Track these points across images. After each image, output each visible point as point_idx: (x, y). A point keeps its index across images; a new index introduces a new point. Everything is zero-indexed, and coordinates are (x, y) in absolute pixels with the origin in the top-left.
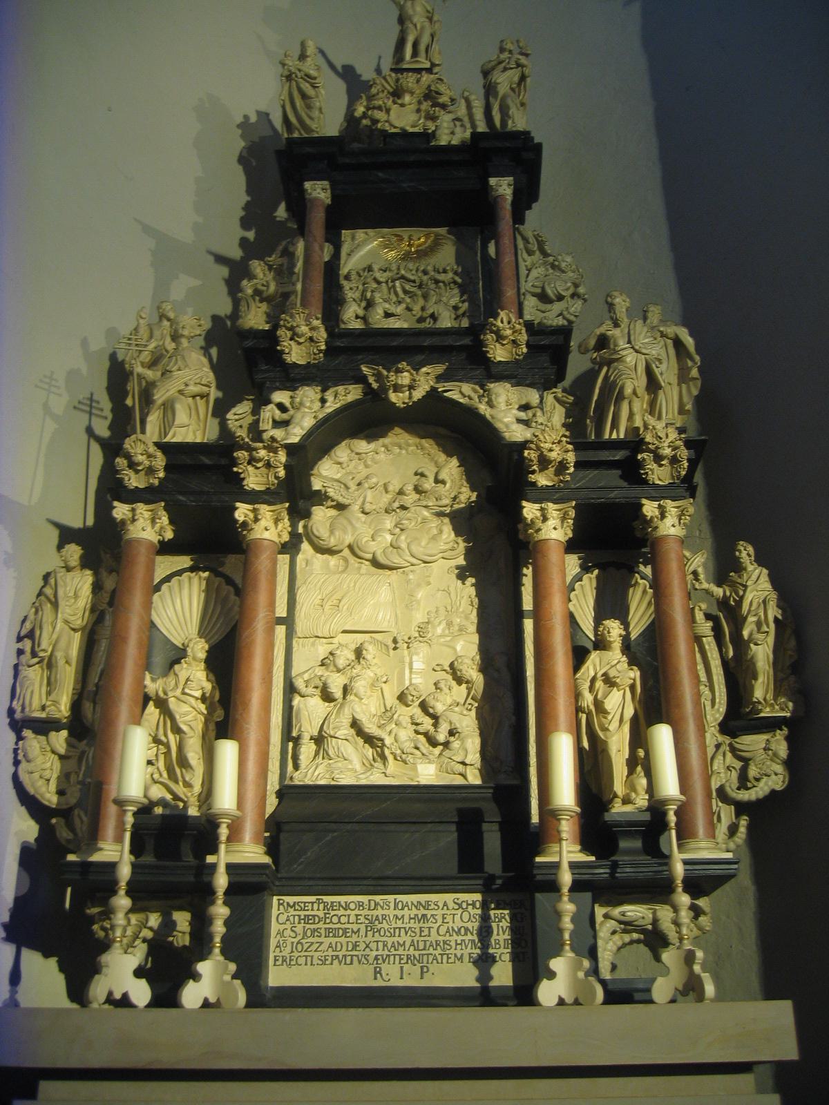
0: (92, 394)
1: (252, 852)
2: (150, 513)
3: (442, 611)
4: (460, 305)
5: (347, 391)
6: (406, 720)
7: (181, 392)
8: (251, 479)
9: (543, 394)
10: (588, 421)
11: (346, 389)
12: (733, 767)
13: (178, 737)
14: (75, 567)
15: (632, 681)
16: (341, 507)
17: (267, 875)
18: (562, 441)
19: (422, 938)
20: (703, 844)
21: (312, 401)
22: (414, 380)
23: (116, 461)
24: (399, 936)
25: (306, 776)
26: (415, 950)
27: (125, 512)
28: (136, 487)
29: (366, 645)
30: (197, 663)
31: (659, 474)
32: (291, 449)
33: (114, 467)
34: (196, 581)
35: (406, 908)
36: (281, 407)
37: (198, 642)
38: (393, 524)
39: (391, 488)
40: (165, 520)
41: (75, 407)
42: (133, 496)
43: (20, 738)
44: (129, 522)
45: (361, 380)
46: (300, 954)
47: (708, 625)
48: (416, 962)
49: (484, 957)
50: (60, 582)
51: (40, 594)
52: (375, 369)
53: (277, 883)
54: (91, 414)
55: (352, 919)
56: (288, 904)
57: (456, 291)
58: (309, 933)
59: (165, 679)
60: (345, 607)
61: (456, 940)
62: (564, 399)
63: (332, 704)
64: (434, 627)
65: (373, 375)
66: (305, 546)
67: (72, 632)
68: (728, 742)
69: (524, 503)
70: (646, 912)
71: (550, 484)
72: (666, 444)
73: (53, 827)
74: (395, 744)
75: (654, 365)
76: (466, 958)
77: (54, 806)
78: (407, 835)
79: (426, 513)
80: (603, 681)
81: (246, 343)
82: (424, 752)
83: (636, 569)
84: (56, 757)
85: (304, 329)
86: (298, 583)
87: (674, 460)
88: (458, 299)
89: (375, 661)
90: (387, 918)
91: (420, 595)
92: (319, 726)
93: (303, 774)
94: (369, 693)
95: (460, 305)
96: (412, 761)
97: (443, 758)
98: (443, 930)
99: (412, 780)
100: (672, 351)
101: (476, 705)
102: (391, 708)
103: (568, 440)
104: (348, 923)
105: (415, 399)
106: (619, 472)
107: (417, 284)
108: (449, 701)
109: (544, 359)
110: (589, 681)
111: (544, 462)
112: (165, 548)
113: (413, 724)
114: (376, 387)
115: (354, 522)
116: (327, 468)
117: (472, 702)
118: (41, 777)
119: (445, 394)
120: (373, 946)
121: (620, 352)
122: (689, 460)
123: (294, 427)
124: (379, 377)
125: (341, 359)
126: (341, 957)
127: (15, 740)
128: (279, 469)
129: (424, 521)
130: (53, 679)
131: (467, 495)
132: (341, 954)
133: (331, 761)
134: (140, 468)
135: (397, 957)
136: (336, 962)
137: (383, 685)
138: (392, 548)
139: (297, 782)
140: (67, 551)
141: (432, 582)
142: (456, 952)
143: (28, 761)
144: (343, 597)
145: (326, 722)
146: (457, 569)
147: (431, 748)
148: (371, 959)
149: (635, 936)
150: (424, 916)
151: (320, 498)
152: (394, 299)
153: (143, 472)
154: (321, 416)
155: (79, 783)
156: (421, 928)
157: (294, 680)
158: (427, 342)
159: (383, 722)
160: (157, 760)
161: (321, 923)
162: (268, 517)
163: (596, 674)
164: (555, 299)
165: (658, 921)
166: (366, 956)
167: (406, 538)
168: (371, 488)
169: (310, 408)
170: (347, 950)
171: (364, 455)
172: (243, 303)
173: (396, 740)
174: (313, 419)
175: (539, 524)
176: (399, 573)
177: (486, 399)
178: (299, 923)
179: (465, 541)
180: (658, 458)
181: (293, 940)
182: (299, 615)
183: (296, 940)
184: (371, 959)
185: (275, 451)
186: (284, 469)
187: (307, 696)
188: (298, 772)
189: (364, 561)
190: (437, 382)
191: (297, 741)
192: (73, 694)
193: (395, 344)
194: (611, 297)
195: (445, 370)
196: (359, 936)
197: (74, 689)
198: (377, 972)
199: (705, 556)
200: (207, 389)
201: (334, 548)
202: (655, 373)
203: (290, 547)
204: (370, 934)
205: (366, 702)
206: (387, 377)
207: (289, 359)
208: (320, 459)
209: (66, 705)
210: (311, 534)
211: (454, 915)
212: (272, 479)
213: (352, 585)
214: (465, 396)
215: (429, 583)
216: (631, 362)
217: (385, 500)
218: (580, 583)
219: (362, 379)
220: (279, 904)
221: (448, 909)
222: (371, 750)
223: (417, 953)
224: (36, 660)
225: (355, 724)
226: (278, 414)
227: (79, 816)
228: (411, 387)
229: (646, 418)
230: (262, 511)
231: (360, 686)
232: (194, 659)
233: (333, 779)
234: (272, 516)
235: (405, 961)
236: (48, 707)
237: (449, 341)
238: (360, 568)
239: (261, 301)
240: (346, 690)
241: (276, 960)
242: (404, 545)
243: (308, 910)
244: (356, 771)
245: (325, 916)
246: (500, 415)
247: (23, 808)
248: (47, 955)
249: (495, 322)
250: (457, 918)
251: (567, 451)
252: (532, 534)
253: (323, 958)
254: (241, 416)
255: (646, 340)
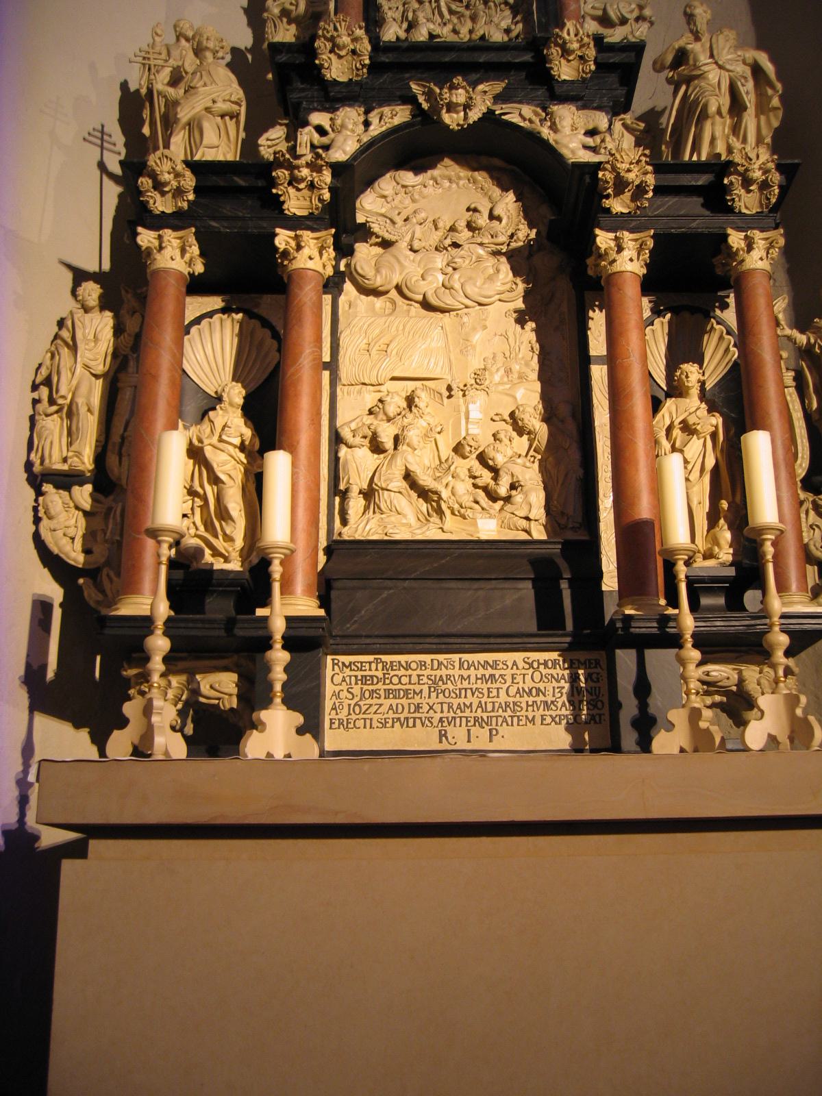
0: (103, 126)
1: (306, 606)
2: (178, 241)
3: (500, 358)
4: (513, 27)
5: (394, 113)
6: (463, 473)
7: (207, 109)
8: (292, 202)
9: (612, 118)
10: (663, 147)
11: (393, 110)
12: (817, 526)
13: (215, 488)
14: (93, 308)
15: (714, 429)
16: (386, 244)
17: (323, 629)
18: (641, 161)
19: (490, 700)
20: (796, 599)
21: (355, 124)
22: (471, 98)
23: (139, 181)
24: (466, 697)
25: (356, 531)
26: (483, 712)
27: (151, 239)
28: (163, 212)
29: (418, 392)
30: (234, 409)
31: (747, 202)
32: (338, 169)
33: (137, 188)
34: (228, 323)
35: (472, 668)
36: (321, 131)
37: (235, 386)
38: (445, 263)
39: (441, 225)
40: (195, 250)
41: (84, 139)
42: (158, 222)
43: (39, 493)
44: (155, 251)
46: (357, 717)
47: (790, 374)
48: (484, 725)
49: (557, 719)
50: (77, 323)
51: (56, 337)
52: (424, 86)
53: (332, 641)
54: (102, 147)
55: (415, 679)
56: (343, 663)
57: (508, 12)
58: (367, 695)
59: (199, 426)
60: (394, 352)
61: (527, 702)
62: (635, 125)
63: (382, 456)
64: (492, 374)
65: (424, 93)
66: (348, 286)
67: (94, 379)
68: (811, 499)
69: (598, 231)
70: (732, 672)
71: (625, 211)
72: (756, 166)
73: (80, 588)
74: (453, 497)
75: (739, 84)
76: (538, 720)
77: (80, 566)
78: (470, 592)
79: (481, 251)
80: (681, 429)
81: (279, 57)
82: (485, 506)
83: (712, 314)
84: (80, 513)
85: (345, 40)
86: (341, 326)
87: (764, 185)
88: (510, 21)
89: (428, 410)
90: (452, 679)
91: (477, 337)
92: (370, 476)
93: (354, 530)
94: (422, 444)
95: (513, 27)
96: (471, 515)
97: (504, 514)
98: (513, 691)
99: (472, 536)
101: (540, 457)
102: (446, 460)
103: (648, 160)
104: (410, 683)
105: (471, 122)
106: (701, 200)
107: (464, 4)
108: (509, 453)
109: (613, 79)
110: (664, 429)
111: (621, 185)
112: (196, 286)
113: (470, 477)
114: (426, 108)
115: (402, 259)
116: (370, 201)
117: (536, 455)
118: (65, 535)
119: (503, 117)
120: (437, 707)
121: (702, 68)
122: (780, 187)
123: (336, 151)
124: (430, 95)
125: (386, 77)
126: (402, 720)
127: (34, 497)
128: (324, 191)
129: (479, 259)
130: (74, 428)
131: (525, 233)
132: (402, 717)
133: (383, 516)
134: (166, 189)
135: (464, 720)
136: (397, 725)
137: (438, 436)
138: (443, 289)
139: (346, 538)
140: (84, 290)
141: (488, 325)
142: (526, 713)
143: (50, 518)
144: (391, 341)
145: (377, 474)
146: (515, 312)
147: (491, 503)
148: (435, 721)
149: (718, 698)
150: (492, 676)
151: (364, 232)
152: (439, 20)
153: (170, 195)
154: (365, 139)
155: (106, 541)
156: (488, 689)
157: (339, 430)
158: (483, 58)
159: (438, 474)
160: (193, 514)
161: (380, 684)
162: (312, 245)
163: (672, 423)
164: (617, 21)
165: (744, 681)
166: (430, 719)
167: (459, 280)
168: (421, 224)
169: (353, 131)
170: (409, 712)
171: (411, 188)
172: (270, 25)
173: (453, 494)
174: (356, 143)
175: (613, 255)
176: (452, 316)
177: (549, 124)
178: (356, 684)
179: (524, 281)
180: (747, 183)
181: (350, 702)
182: (343, 361)
183: (353, 702)
184: (435, 721)
185: (319, 170)
186: (329, 191)
187: (355, 447)
188: (347, 528)
189: (413, 303)
190: (495, 103)
191: (344, 495)
192: (96, 446)
193: (447, 59)
194: (690, 7)
195: (504, 89)
196: (421, 698)
197: (97, 441)
198: (443, 735)
199: (786, 301)
200: (236, 107)
201: (380, 288)
202: (741, 93)
203: (333, 285)
204: (433, 695)
205: (419, 454)
206: (440, 94)
207: (328, 76)
208: (363, 191)
209: (89, 458)
210: (354, 273)
211: (524, 675)
212: (315, 202)
213: (401, 328)
214: (524, 119)
215: (485, 327)
216: (714, 79)
217: (435, 237)
218: (650, 327)
219: (411, 100)
220: (334, 664)
221: (517, 668)
222: (425, 505)
223: (485, 716)
224: (55, 408)
225: (408, 476)
226: (316, 135)
227: (108, 575)
228: (467, 107)
229: (730, 141)
230: (305, 238)
231: (413, 435)
232: (231, 404)
233: (386, 534)
234: (317, 243)
235: (472, 723)
236: (70, 458)
237: (507, 57)
238: (409, 311)
239: (289, 23)
240: (397, 439)
241: (331, 723)
242: (457, 286)
243: (365, 670)
244: (411, 526)
245: (384, 676)
246: (565, 141)
247: (46, 570)
248: (77, 726)
249: (560, 33)
250: (528, 678)
251: (646, 173)
252: (605, 266)
253: (383, 721)
254: (277, 141)
255: (729, 57)
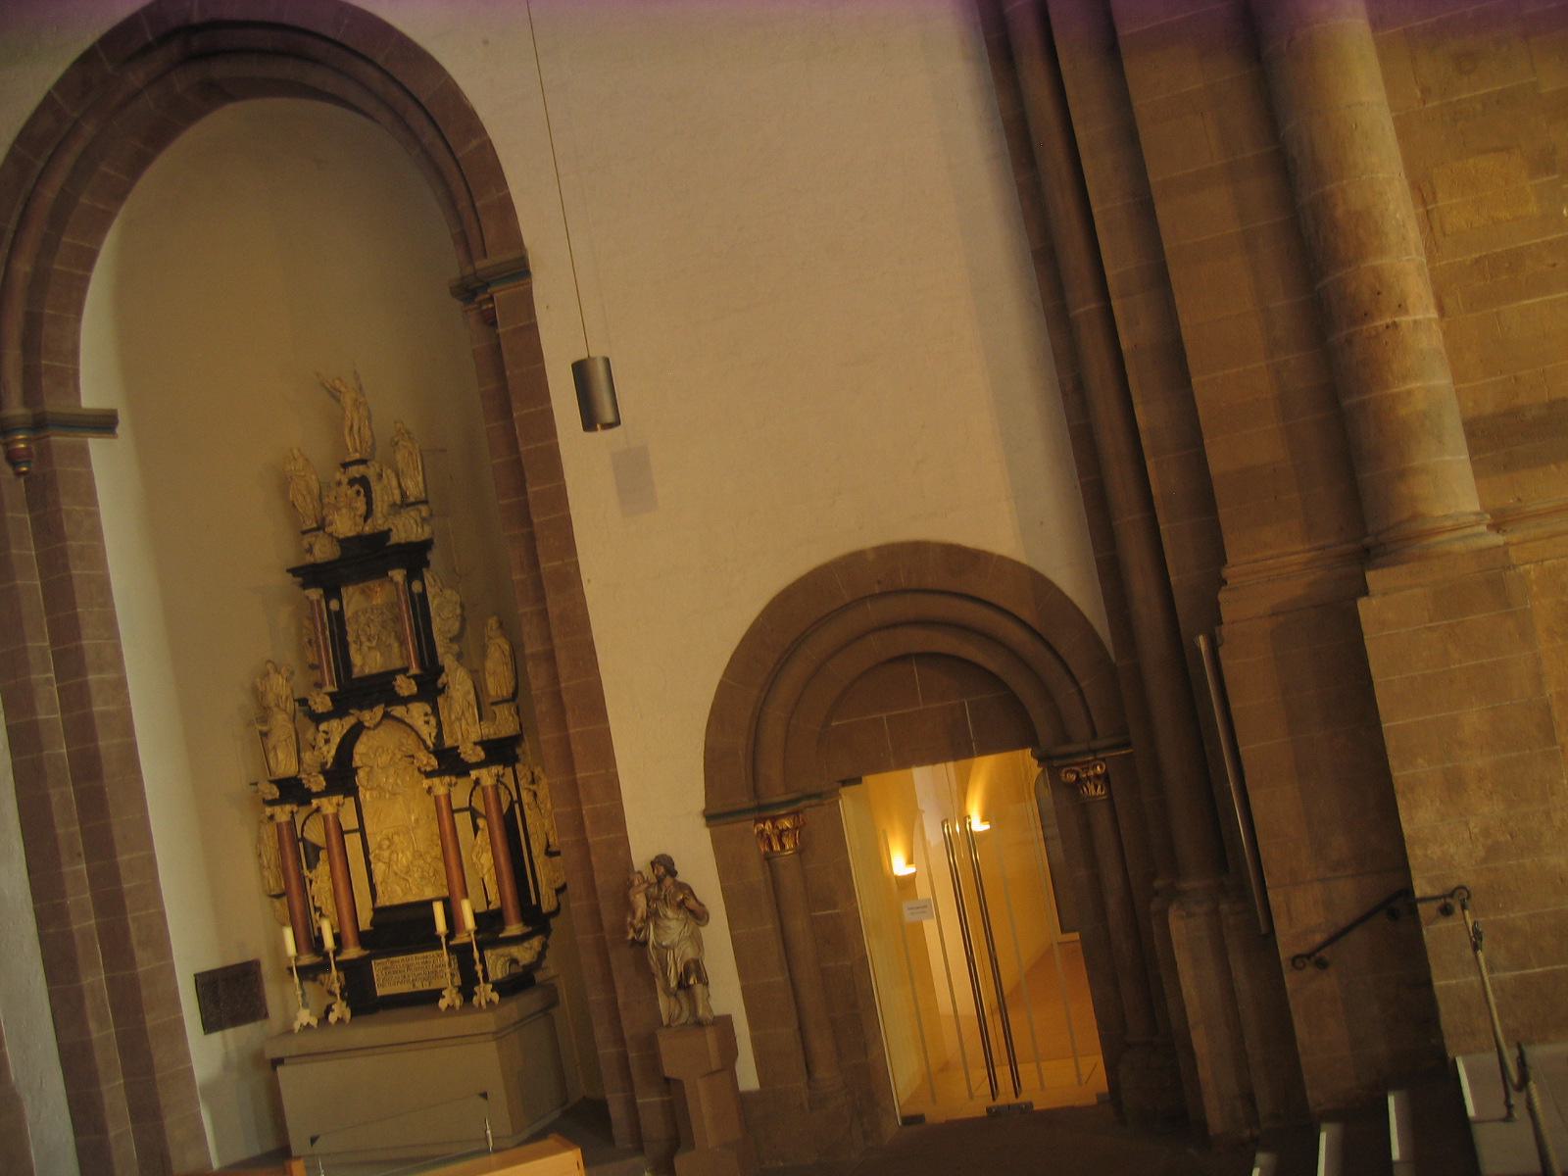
36: (326, 732)
45: (353, 714)
100: (497, 654)
198: (414, 985)
226: (324, 735)
